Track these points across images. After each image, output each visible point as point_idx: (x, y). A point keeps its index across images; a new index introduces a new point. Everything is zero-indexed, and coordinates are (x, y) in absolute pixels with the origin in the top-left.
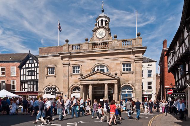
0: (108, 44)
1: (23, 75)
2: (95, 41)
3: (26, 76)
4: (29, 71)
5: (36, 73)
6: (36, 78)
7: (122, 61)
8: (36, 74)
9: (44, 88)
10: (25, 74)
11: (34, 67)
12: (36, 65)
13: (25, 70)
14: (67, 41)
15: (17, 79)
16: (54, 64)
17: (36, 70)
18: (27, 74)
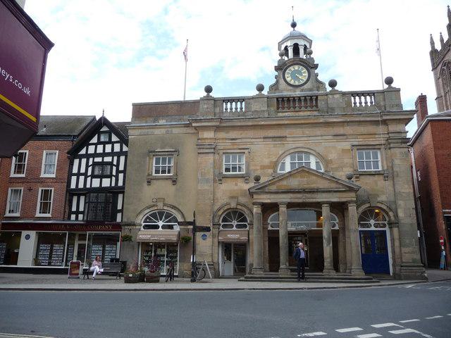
0: (317, 99)
1: (78, 174)
2: (282, 92)
3: (86, 177)
4: (95, 164)
5: (114, 168)
6: (113, 185)
7: (356, 143)
8: (114, 173)
9: (140, 213)
10: (83, 170)
11: (112, 154)
12: (117, 148)
13: (84, 161)
14: (209, 89)
15: (58, 185)
16: (171, 147)
17: (115, 163)
18: (89, 173)
